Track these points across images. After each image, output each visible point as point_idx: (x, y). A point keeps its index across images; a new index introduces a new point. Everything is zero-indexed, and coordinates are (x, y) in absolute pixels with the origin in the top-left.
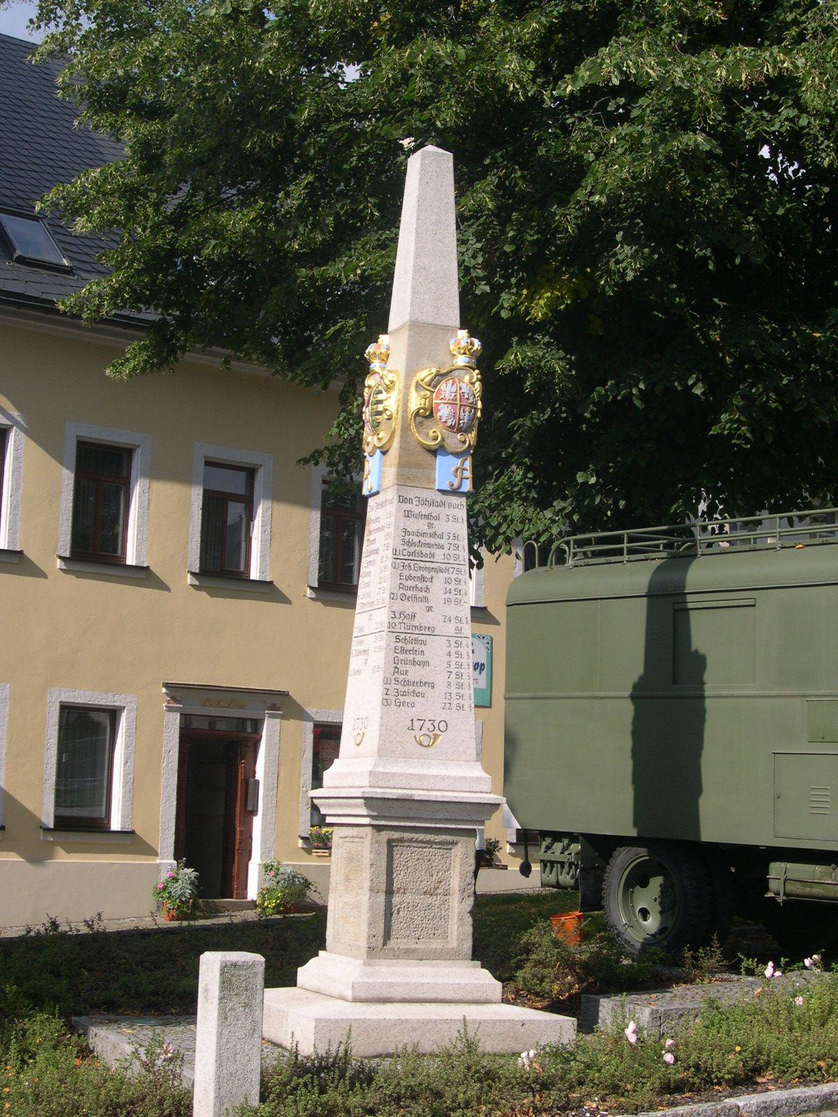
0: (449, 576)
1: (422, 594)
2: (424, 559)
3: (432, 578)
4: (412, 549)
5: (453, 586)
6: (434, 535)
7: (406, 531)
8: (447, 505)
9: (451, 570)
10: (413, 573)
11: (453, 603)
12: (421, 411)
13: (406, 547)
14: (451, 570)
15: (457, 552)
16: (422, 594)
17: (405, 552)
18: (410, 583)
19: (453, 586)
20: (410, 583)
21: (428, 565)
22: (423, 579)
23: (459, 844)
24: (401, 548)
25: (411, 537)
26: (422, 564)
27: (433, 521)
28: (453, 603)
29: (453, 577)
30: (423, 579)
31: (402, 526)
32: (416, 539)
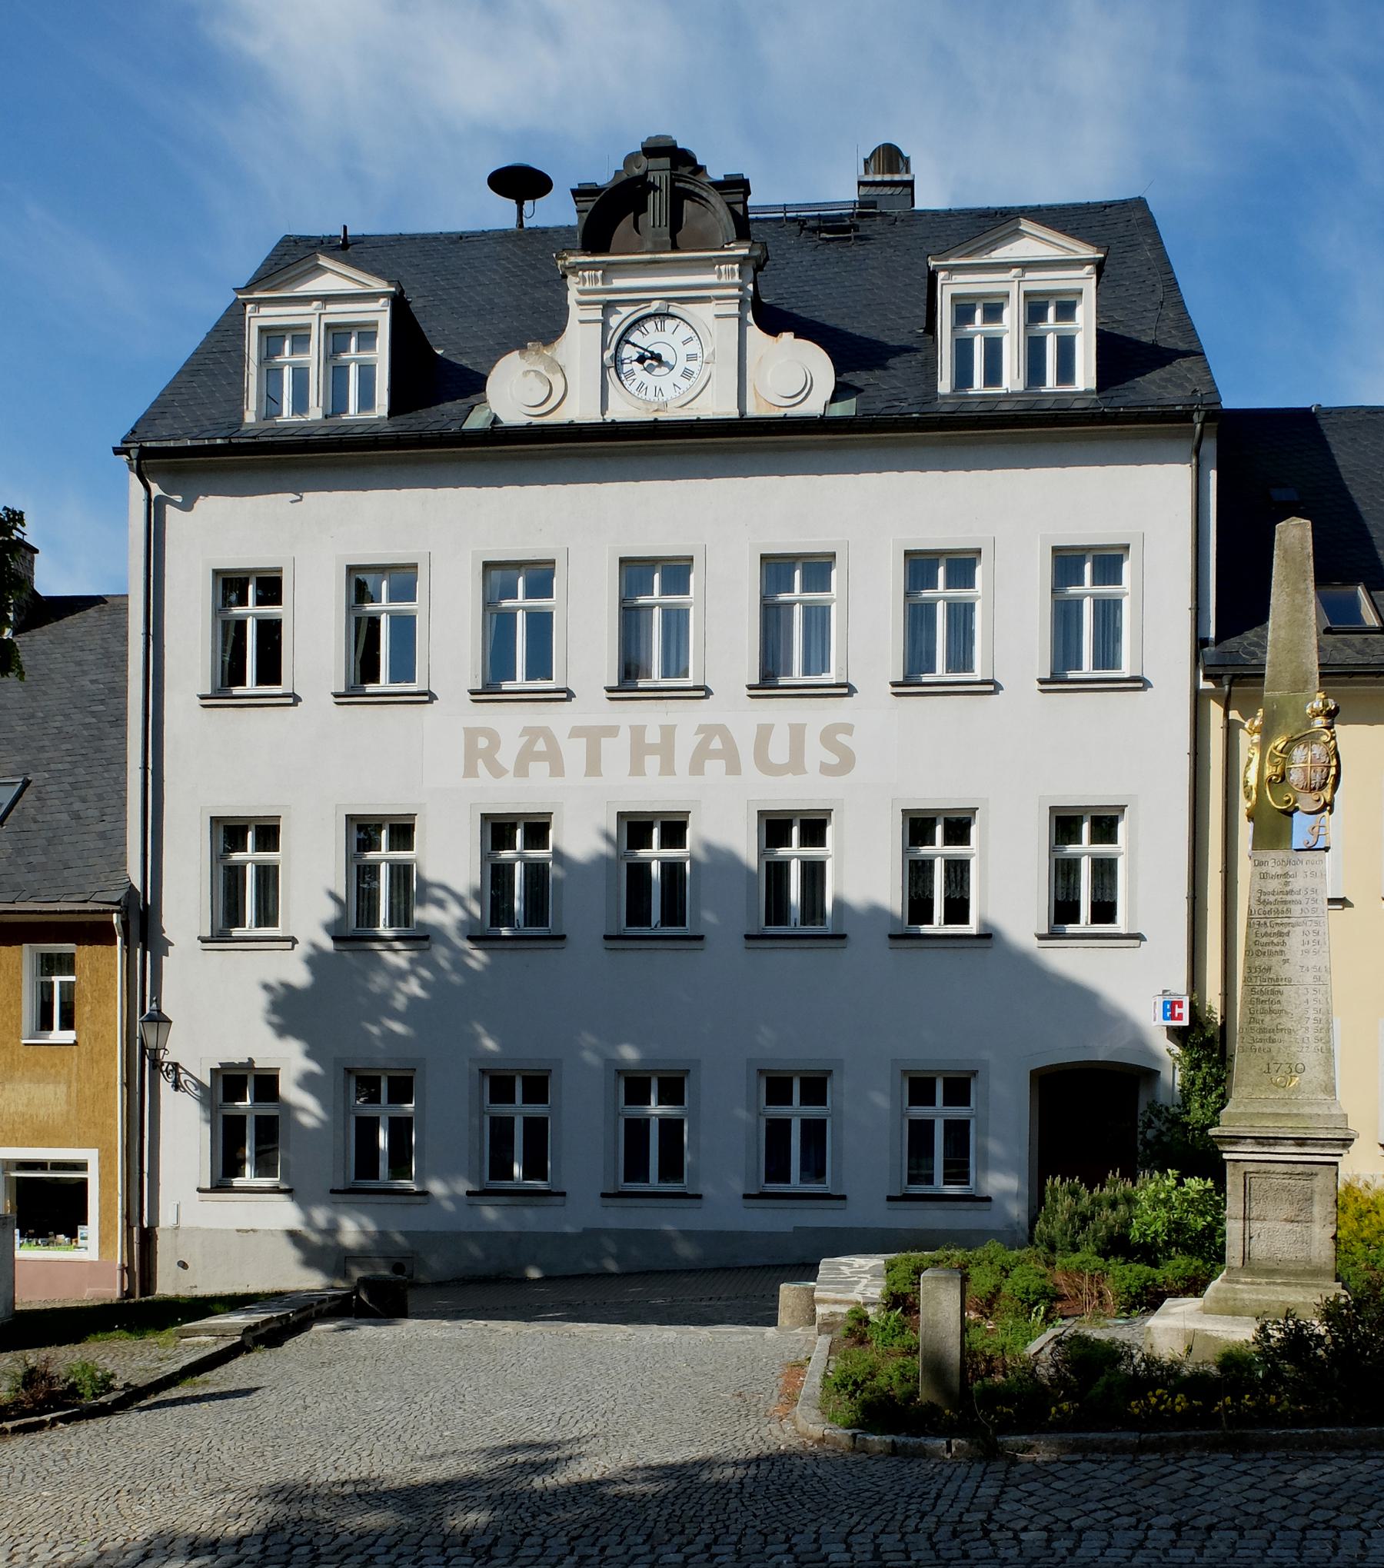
0: (1308, 928)
1: (1278, 948)
2: (1280, 916)
3: (1289, 932)
4: (1268, 908)
5: (1311, 937)
6: (1291, 892)
7: (1261, 892)
8: (1304, 863)
9: (1309, 923)
10: (1269, 930)
11: (1311, 953)
12: (1274, 778)
13: (1261, 907)
14: (1309, 923)
15: (1315, 906)
16: (1278, 948)
17: (1261, 912)
18: (1265, 940)
19: (1311, 937)
20: (1265, 940)
21: (1286, 920)
22: (1280, 934)
23: (1319, 1176)
24: (1257, 908)
25: (1267, 897)
26: (1279, 921)
27: (1290, 879)
28: (1311, 953)
29: (1311, 929)
30: (1280, 934)
31: (1257, 887)
32: (1272, 898)
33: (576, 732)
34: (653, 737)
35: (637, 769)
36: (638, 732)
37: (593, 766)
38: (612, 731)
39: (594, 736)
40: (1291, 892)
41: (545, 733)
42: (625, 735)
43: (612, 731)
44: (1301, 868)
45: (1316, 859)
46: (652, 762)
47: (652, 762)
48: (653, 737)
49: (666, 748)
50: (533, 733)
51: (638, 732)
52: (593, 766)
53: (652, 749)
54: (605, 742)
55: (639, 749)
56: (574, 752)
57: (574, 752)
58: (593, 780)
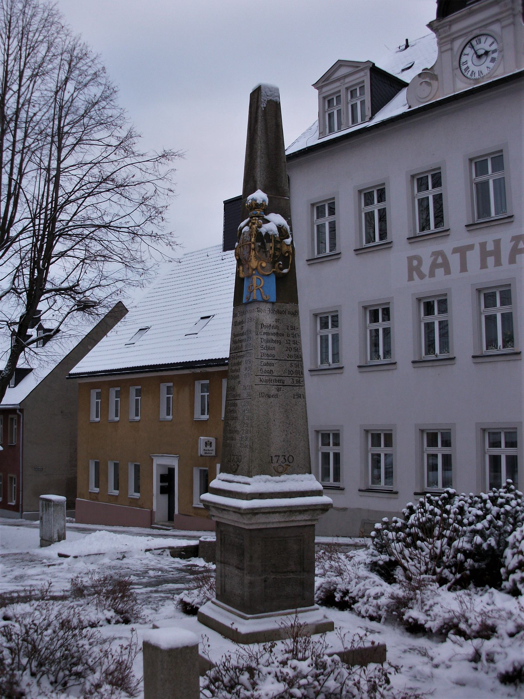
21: (241, 354)
33: (455, 250)
34: (490, 247)
35: (484, 265)
36: (483, 245)
37: (464, 268)
38: (471, 247)
39: (462, 251)
40: (242, 334)
41: (440, 253)
42: (477, 248)
43: (471, 247)
44: (248, 315)
45: (252, 309)
46: (491, 260)
47: (491, 260)
48: (490, 247)
49: (497, 253)
50: (437, 254)
51: (483, 245)
52: (464, 268)
53: (490, 254)
54: (468, 253)
55: (484, 254)
56: (454, 260)
57: (454, 260)
58: (464, 274)
